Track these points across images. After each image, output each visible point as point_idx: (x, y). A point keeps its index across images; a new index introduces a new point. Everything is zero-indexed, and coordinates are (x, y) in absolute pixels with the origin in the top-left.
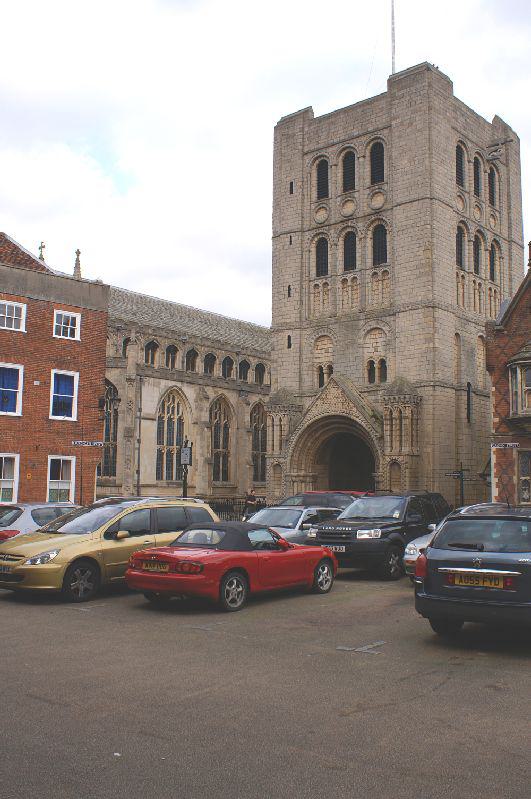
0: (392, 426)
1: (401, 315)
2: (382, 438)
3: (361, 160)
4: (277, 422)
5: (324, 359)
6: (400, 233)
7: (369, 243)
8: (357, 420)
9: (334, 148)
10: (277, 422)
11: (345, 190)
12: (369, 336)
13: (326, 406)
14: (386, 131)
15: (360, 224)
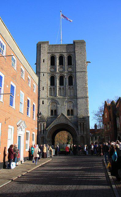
0: (81, 127)
1: (79, 99)
2: (78, 130)
4: (42, 125)
10: (42, 125)
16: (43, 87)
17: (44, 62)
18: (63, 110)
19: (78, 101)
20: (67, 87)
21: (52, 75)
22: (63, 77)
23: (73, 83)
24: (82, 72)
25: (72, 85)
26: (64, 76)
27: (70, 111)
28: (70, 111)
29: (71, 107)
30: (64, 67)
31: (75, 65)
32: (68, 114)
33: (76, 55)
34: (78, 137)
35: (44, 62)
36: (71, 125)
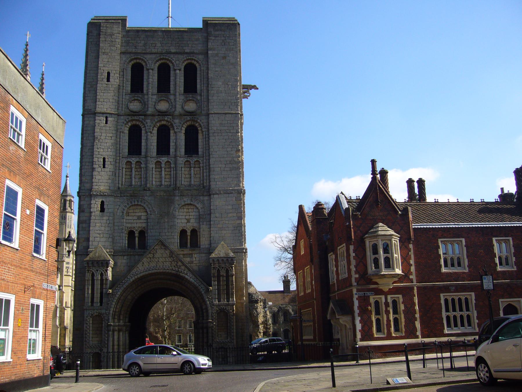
0: (219, 281)
1: (216, 196)
3: (178, 71)
5: (138, 225)
6: (215, 134)
7: (182, 137)
8: (186, 276)
9: (154, 56)
13: (153, 264)
15: (177, 121)
16: (104, 159)
17: (108, 80)
18: (166, 231)
19: (212, 204)
20: (181, 161)
21: (134, 122)
22: (169, 130)
23: (200, 147)
24: (227, 115)
25: (197, 153)
27: (189, 233)
28: (189, 233)
29: (192, 221)
30: (172, 97)
31: (205, 91)
32: (183, 244)
33: (211, 61)
34: (210, 314)
35: (108, 80)
36: (189, 277)
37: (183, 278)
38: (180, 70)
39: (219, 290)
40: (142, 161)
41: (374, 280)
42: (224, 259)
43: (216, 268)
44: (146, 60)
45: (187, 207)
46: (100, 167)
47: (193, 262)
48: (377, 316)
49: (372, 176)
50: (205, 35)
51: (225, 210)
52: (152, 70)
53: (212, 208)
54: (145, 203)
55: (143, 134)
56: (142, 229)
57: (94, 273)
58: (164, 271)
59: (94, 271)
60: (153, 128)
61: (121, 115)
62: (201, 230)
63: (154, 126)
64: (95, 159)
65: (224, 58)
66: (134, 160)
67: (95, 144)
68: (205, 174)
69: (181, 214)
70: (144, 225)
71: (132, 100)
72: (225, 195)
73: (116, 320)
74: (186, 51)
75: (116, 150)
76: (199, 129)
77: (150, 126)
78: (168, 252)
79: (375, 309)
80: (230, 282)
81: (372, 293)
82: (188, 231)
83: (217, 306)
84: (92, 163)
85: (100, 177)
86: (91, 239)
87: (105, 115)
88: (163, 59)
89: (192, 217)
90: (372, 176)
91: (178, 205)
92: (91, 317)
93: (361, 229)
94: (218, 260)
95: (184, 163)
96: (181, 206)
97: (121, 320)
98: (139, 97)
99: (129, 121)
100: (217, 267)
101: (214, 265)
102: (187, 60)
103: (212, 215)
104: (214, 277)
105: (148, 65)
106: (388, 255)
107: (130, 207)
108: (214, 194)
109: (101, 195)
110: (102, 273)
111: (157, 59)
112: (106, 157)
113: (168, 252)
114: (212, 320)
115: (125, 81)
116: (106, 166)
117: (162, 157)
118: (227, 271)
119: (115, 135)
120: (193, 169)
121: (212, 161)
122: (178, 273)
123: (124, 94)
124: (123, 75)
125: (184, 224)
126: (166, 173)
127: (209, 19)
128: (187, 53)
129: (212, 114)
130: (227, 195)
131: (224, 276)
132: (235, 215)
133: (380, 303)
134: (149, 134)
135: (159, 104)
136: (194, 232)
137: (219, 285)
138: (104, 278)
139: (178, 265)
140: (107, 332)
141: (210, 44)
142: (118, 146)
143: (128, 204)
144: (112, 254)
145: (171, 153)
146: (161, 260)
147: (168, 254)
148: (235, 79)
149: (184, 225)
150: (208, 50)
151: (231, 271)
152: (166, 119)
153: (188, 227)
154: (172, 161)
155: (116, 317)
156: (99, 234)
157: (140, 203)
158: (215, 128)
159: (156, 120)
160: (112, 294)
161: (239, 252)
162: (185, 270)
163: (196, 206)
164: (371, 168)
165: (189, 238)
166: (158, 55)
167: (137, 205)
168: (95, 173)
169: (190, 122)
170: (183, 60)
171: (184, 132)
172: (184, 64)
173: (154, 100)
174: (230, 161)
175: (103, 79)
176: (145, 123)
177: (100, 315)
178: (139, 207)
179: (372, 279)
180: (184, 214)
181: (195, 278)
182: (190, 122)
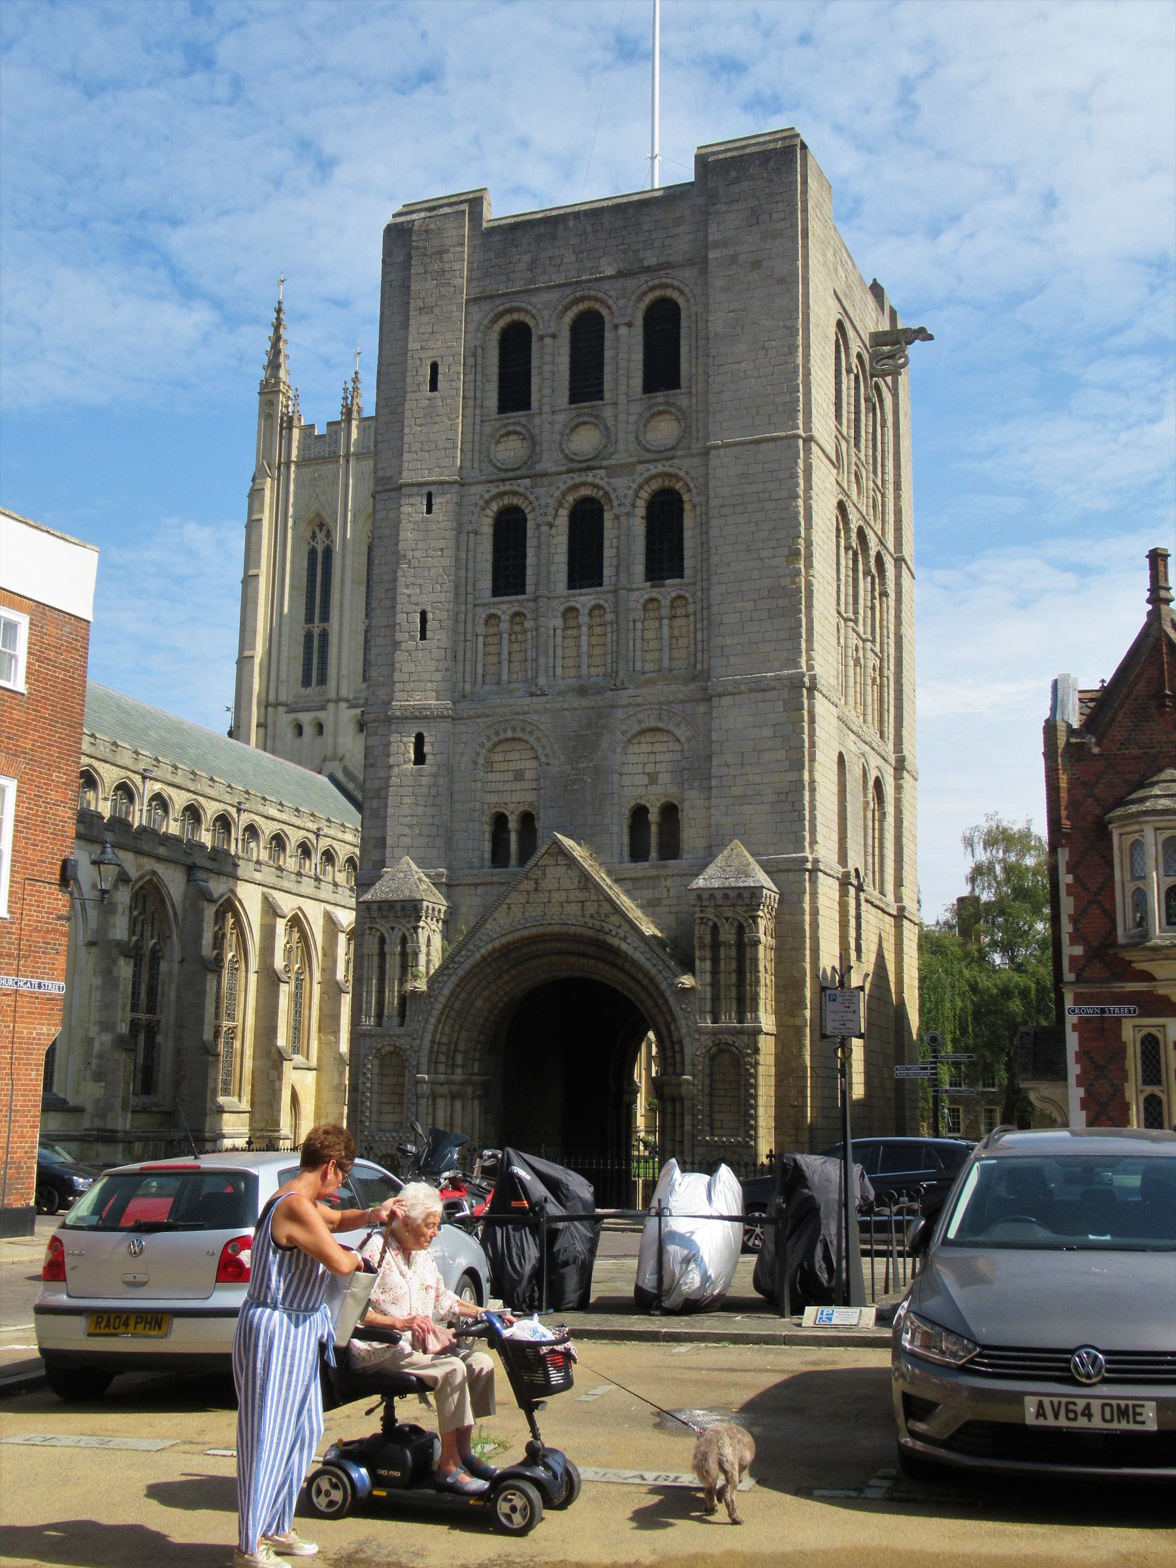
0: (715, 960)
1: (727, 700)
3: (623, 330)
6: (724, 511)
7: (638, 527)
8: (624, 946)
9: (554, 295)
11: (576, 396)
12: (631, 749)
14: (689, 274)
16: (423, 615)
17: (434, 387)
19: (715, 725)
21: (506, 501)
22: (601, 511)
23: (687, 553)
26: (611, 501)
27: (653, 816)
28: (653, 816)
29: (664, 778)
34: (688, 1060)
35: (434, 387)
37: (617, 952)
38: (629, 325)
39: (715, 985)
40: (526, 612)
41: (1139, 966)
42: (729, 892)
43: (709, 919)
44: (534, 311)
45: (648, 738)
46: (412, 638)
47: (659, 899)
48: (1149, 1089)
49: (1150, 607)
50: (700, 201)
51: (751, 742)
52: (554, 336)
53: (714, 736)
54: (531, 733)
55: (529, 533)
56: (526, 808)
57: (386, 935)
58: (564, 929)
59: (384, 931)
60: (557, 511)
61: (471, 484)
62: (686, 805)
63: (560, 505)
64: (401, 618)
65: (757, 265)
66: (506, 606)
67: (400, 574)
68: (699, 636)
69: (632, 759)
70: (531, 797)
71: (503, 436)
72: (753, 695)
73: (442, 1068)
74: (646, 264)
75: (457, 586)
76: (685, 497)
77: (547, 506)
78: (574, 873)
79: (1143, 1062)
80: (748, 962)
81: (1132, 1007)
82: (651, 810)
83: (708, 1033)
84: (392, 626)
85: (412, 668)
86: (389, 841)
87: (425, 490)
88: (583, 299)
89: (659, 768)
90: (1150, 607)
91: (623, 733)
92: (375, 1057)
93: (1096, 791)
94: (712, 897)
95: (672, 602)
96: (628, 735)
97: (457, 1066)
98: (519, 423)
99: (493, 498)
100: (711, 917)
101: (701, 911)
102: (652, 289)
103: (715, 761)
104: (702, 947)
105: (541, 326)
106: (1140, 884)
107: (495, 745)
108: (720, 696)
109: (416, 718)
110: (382, 934)
111: (564, 303)
112: (429, 609)
113: (574, 873)
114: (693, 1075)
115: (478, 383)
116: (429, 634)
117: (581, 595)
118: (741, 930)
119: (452, 544)
120: (666, 622)
121: (716, 591)
122: (601, 936)
123: (478, 420)
124: (476, 366)
125: (639, 789)
126: (594, 640)
127: (710, 150)
128: (647, 270)
129: (717, 447)
130: (760, 696)
131: (730, 946)
132: (781, 755)
133: (1162, 1045)
134: (544, 529)
135: (574, 436)
136: (528, 820)
137: (715, 972)
138: (409, 950)
139: (602, 911)
140: (414, 1100)
141: (712, 228)
142: (462, 573)
143: (489, 738)
144: (444, 880)
145: (606, 580)
146: (557, 897)
147: (576, 881)
148: (788, 328)
149: (641, 791)
150: (706, 247)
151: (751, 929)
152: (590, 479)
153: (652, 798)
154: (607, 601)
155: (442, 1058)
156: (410, 826)
157: (519, 734)
158: (725, 492)
159: (563, 487)
160: (430, 996)
161: (791, 870)
162: (619, 927)
163: (672, 733)
164: (1148, 580)
165: (654, 829)
166: (568, 291)
167: (514, 739)
168: (400, 656)
169: (660, 481)
170: (639, 291)
171: (641, 511)
172: (643, 305)
173: (558, 427)
174: (769, 590)
175: (419, 385)
176: (532, 498)
177: (397, 1052)
178: (520, 746)
179: (1132, 962)
180: (642, 759)
181: (647, 949)
182: (660, 481)
